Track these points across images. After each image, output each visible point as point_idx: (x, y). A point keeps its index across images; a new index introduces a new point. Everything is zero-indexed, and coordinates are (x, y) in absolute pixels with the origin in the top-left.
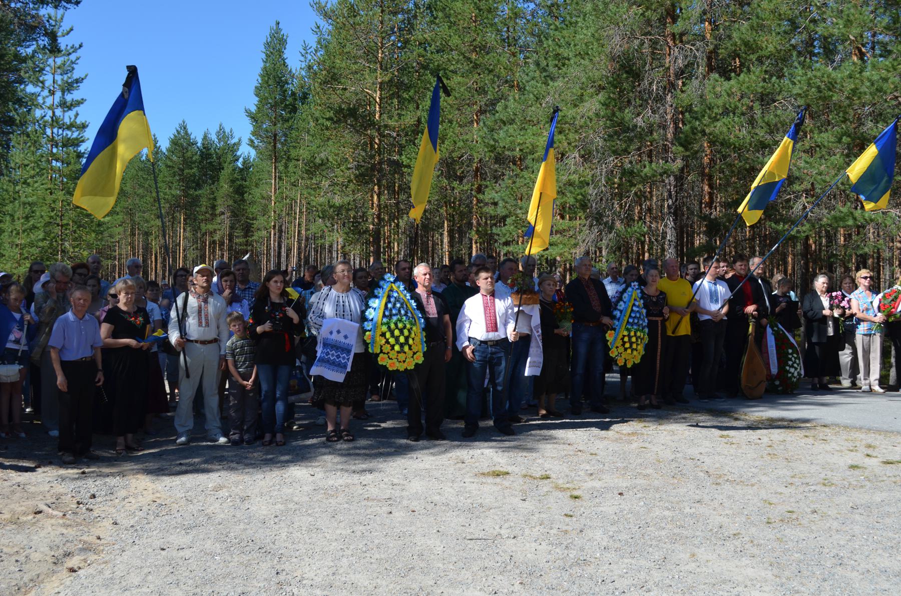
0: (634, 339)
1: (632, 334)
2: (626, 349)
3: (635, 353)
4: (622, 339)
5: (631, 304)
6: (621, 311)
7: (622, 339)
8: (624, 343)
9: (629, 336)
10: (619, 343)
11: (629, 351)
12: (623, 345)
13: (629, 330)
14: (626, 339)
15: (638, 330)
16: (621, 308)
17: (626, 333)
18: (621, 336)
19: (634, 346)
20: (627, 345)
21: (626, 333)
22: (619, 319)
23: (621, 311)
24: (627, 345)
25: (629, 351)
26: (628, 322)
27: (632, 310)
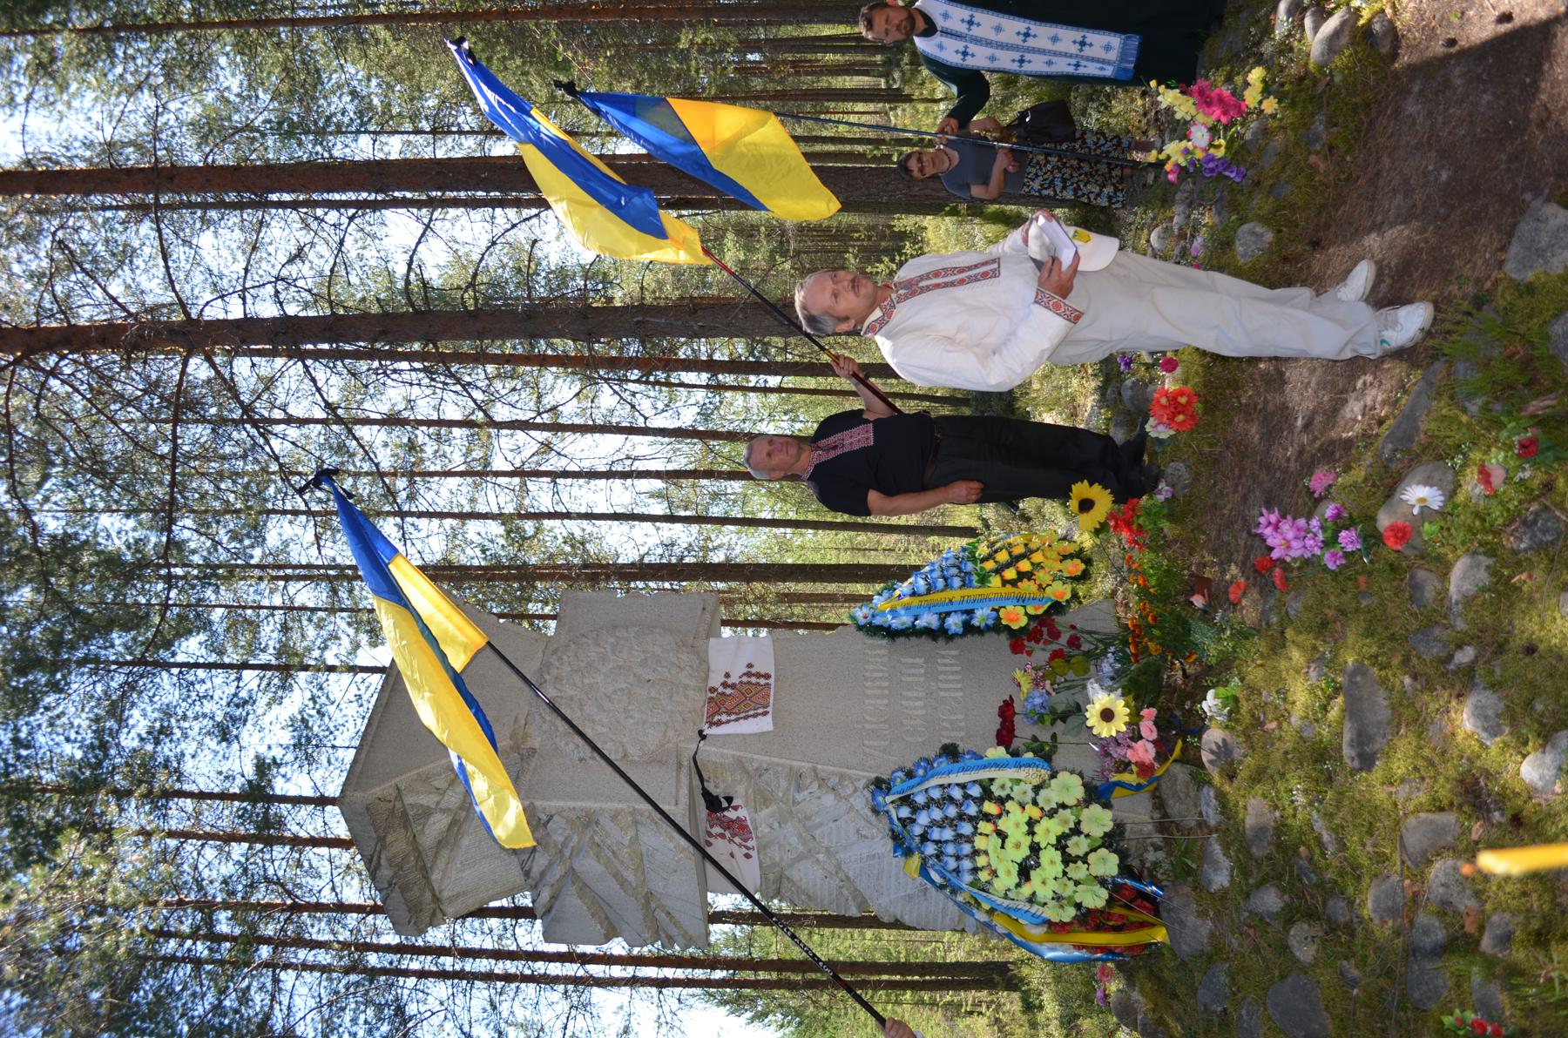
0: (1003, 557)
1: (990, 565)
2: (1038, 566)
4: (1014, 583)
5: (916, 601)
6: (943, 616)
7: (1014, 583)
8: (1022, 576)
9: (999, 571)
10: (1026, 586)
11: (1037, 557)
12: (1022, 576)
13: (984, 580)
14: (1010, 574)
15: (973, 559)
16: (936, 617)
17: (995, 581)
18: (1009, 587)
19: (1019, 550)
20: (1025, 566)
21: (995, 581)
22: (970, 612)
23: (943, 616)
24: (1025, 566)
25: (1037, 557)
26: (964, 585)
27: (928, 592)
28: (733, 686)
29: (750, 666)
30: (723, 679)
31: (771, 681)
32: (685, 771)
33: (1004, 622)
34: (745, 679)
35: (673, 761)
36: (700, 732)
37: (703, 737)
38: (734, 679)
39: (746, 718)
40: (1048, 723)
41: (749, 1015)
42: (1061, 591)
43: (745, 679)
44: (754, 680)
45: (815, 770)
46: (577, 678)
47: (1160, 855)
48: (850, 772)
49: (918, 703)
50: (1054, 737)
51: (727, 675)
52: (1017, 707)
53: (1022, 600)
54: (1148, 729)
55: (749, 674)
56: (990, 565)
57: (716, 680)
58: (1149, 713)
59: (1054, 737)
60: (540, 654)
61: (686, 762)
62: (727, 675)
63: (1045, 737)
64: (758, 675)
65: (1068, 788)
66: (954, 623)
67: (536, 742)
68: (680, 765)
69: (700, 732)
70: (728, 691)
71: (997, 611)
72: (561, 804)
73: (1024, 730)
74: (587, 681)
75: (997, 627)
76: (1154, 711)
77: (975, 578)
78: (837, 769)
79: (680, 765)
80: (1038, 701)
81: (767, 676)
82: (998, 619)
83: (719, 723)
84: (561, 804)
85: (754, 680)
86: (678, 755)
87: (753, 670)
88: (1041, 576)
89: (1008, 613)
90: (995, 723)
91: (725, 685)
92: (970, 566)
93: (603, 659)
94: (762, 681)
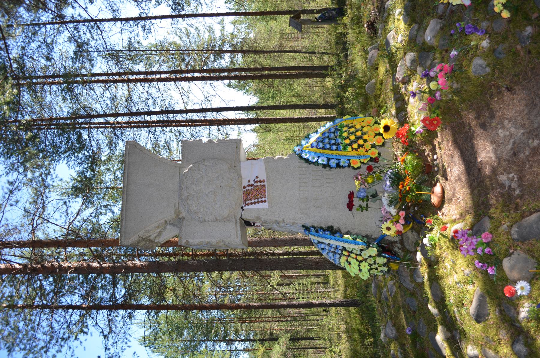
0: (353, 138)
1: (347, 141)
2: (365, 141)
3: (365, 129)
4: (356, 149)
6: (329, 159)
7: (356, 149)
8: (360, 146)
9: (350, 145)
11: (365, 137)
12: (360, 146)
13: (345, 149)
14: (355, 146)
15: (341, 136)
16: (325, 159)
17: (349, 148)
18: (355, 152)
19: (359, 134)
20: (361, 142)
24: (361, 142)
25: (365, 137)
26: (336, 150)
28: (252, 185)
29: (257, 177)
30: (247, 184)
31: (265, 183)
32: (238, 223)
33: (352, 165)
34: (256, 184)
35: (233, 220)
36: (242, 208)
37: (244, 210)
38: (252, 182)
39: (258, 202)
40: (365, 200)
41: (243, 91)
42: (374, 153)
43: (256, 184)
44: (259, 184)
45: (284, 220)
46: (194, 187)
47: (400, 251)
48: (296, 222)
49: (319, 190)
50: (367, 205)
51: (249, 181)
52: (355, 195)
53: (359, 157)
54: (402, 222)
55: (257, 182)
56: (347, 141)
57: (245, 183)
58: (403, 213)
59: (367, 205)
60: (178, 174)
61: (238, 221)
62: (249, 181)
63: (364, 204)
64: (261, 181)
65: (373, 251)
66: (333, 163)
67: (183, 214)
68: (236, 221)
69: (242, 208)
70: (250, 188)
71: (349, 160)
72: (197, 240)
73: (357, 202)
74: (198, 188)
75: (349, 166)
76: (404, 212)
77: (342, 147)
78: (292, 221)
79: (236, 221)
80: (362, 194)
81: (264, 181)
82: (350, 163)
83: (248, 204)
84: (197, 240)
85: (259, 184)
86: (235, 217)
87: (259, 179)
88: (368, 145)
89: (354, 161)
90: (347, 200)
91: (249, 186)
92: (340, 141)
93: (202, 177)
94: (262, 183)
